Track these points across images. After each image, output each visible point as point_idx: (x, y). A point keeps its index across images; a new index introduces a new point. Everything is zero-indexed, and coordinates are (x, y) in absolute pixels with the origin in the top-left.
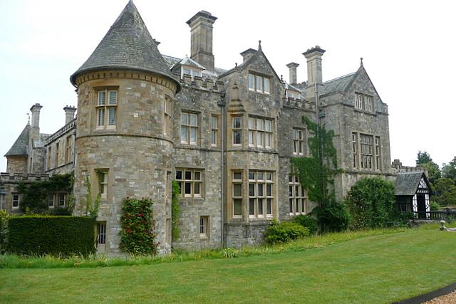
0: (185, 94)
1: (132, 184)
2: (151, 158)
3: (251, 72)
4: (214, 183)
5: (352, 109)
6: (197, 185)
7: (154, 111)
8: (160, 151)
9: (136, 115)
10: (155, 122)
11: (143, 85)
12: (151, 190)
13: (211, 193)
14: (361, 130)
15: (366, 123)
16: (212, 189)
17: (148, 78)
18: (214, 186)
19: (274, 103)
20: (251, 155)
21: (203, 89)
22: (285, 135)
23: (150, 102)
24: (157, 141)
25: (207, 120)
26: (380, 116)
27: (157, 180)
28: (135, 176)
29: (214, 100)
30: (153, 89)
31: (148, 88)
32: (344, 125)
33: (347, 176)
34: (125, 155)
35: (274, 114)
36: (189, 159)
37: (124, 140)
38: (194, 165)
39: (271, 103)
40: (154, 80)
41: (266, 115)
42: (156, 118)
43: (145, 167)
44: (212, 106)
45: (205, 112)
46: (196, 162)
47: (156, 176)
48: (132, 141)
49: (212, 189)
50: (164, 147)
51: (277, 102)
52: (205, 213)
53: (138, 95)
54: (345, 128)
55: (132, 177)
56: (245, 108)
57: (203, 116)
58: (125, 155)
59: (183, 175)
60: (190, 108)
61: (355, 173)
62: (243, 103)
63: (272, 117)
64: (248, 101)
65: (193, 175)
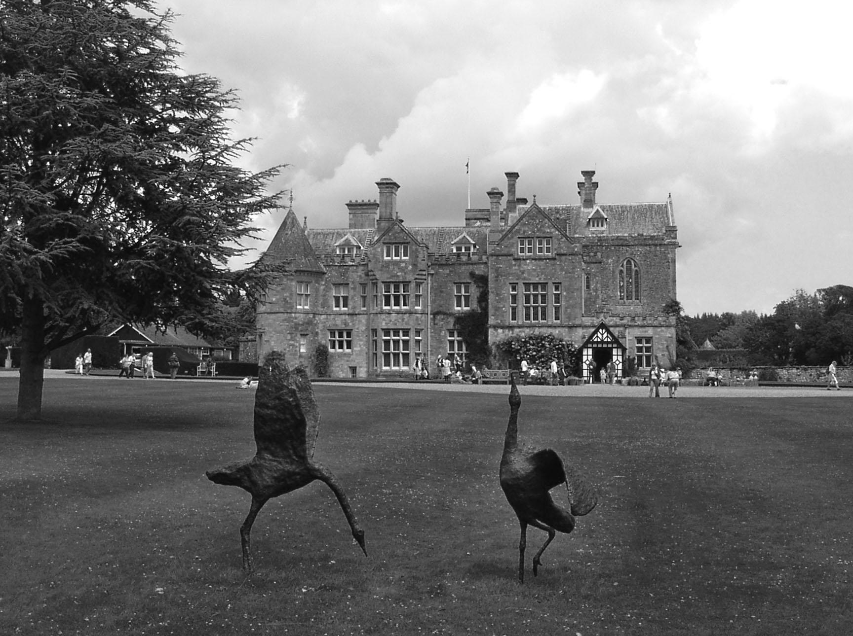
0: (335, 270)
3: (384, 243)
4: (361, 340)
5: (511, 258)
14: (525, 279)
15: (535, 270)
16: (360, 345)
18: (362, 343)
19: (410, 267)
20: (383, 316)
22: (442, 292)
25: (354, 289)
26: (563, 258)
29: (360, 272)
32: (497, 277)
36: (339, 322)
37: (268, 316)
39: (406, 267)
45: (353, 283)
47: (289, 337)
48: (273, 316)
49: (360, 345)
56: (378, 277)
57: (351, 286)
59: (345, 334)
61: (511, 328)
65: (345, 334)
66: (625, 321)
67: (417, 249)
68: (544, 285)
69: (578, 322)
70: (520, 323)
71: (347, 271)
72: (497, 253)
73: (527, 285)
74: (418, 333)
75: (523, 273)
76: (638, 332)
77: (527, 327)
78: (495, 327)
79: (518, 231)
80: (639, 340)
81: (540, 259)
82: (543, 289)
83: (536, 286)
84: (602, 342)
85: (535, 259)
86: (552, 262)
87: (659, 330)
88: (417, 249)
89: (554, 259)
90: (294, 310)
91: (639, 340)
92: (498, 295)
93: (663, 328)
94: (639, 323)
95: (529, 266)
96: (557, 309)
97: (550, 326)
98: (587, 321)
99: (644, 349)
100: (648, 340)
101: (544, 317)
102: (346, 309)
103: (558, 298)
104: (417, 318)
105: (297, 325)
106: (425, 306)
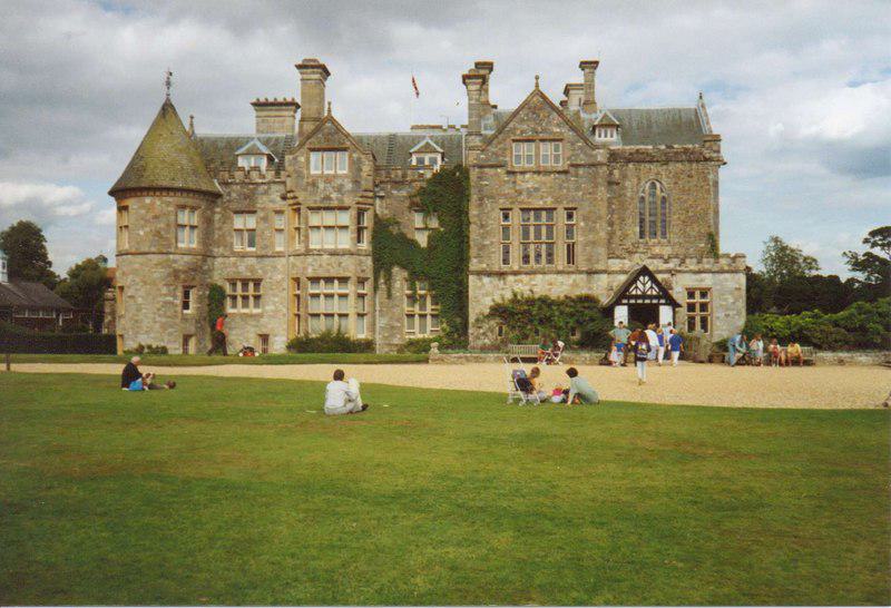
1: (140, 300)
2: (159, 273)
4: (274, 295)
6: (257, 298)
7: (162, 225)
8: (170, 266)
9: (141, 233)
10: (161, 237)
11: (148, 200)
12: (158, 306)
13: (273, 307)
17: (152, 193)
21: (260, 181)
23: (156, 217)
24: (165, 257)
26: (581, 171)
27: (165, 295)
28: (142, 292)
30: (158, 203)
31: (153, 204)
33: (480, 279)
34: (135, 272)
35: (347, 201)
38: (248, 275)
40: (158, 193)
41: (335, 203)
42: (163, 233)
43: (154, 283)
44: (272, 201)
46: (251, 271)
50: (175, 261)
51: (356, 182)
52: (264, 331)
53: (143, 212)
54: (481, 205)
55: (140, 293)
56: (300, 199)
58: (135, 272)
60: (244, 205)
62: (297, 194)
63: (346, 205)
64: (305, 190)
66: (671, 265)
67: (359, 159)
69: (600, 267)
70: (516, 268)
71: (253, 192)
72: (482, 163)
75: (520, 193)
77: (526, 273)
78: (480, 273)
79: (513, 131)
81: (547, 173)
82: (550, 218)
85: (539, 173)
86: (563, 177)
88: (359, 159)
89: (566, 172)
90: (173, 250)
92: (482, 226)
94: (692, 267)
95: (529, 182)
96: (571, 249)
97: (559, 272)
98: (615, 264)
99: (698, 307)
101: (550, 261)
102: (253, 249)
103: (570, 230)
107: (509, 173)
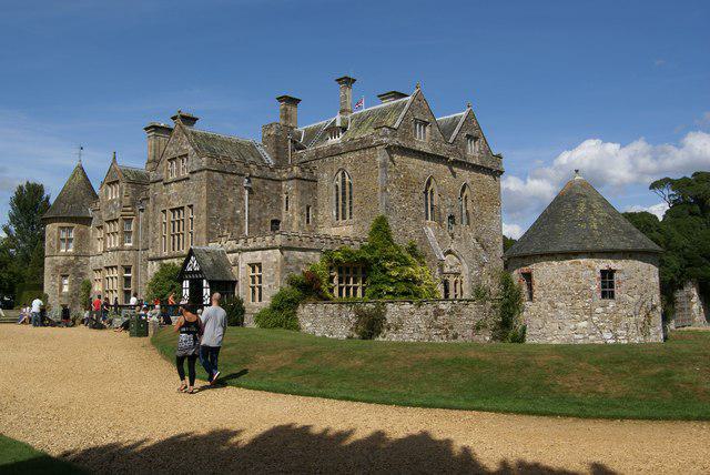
15: (176, 194)
68: (182, 208)
73: (172, 210)
74: (128, 270)
76: (248, 257)
80: (252, 266)
83: (178, 209)
84: (193, 272)
87: (266, 252)
89: (188, 179)
91: (252, 266)
93: (270, 251)
100: (259, 265)
104: (124, 255)
105: (58, 266)
106: (136, 241)
107: (165, 184)
